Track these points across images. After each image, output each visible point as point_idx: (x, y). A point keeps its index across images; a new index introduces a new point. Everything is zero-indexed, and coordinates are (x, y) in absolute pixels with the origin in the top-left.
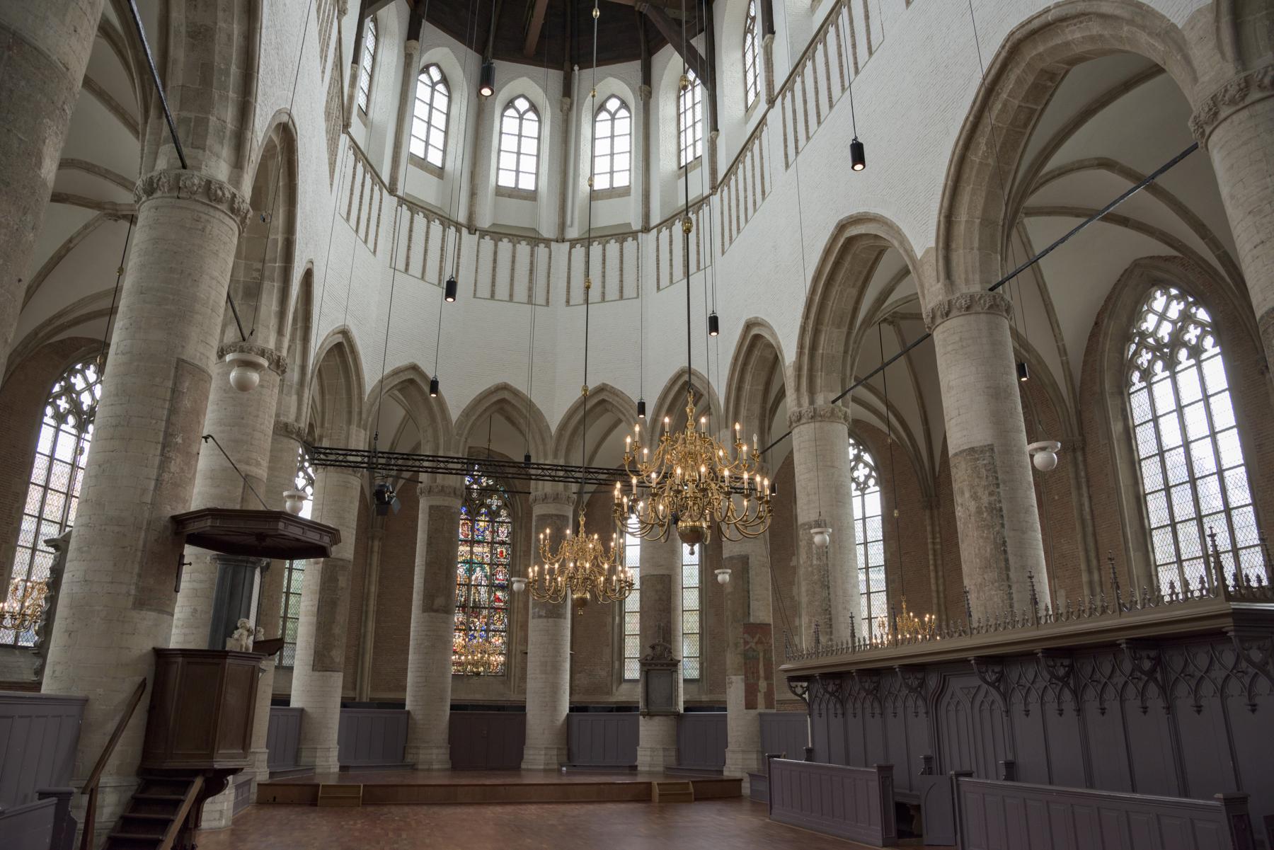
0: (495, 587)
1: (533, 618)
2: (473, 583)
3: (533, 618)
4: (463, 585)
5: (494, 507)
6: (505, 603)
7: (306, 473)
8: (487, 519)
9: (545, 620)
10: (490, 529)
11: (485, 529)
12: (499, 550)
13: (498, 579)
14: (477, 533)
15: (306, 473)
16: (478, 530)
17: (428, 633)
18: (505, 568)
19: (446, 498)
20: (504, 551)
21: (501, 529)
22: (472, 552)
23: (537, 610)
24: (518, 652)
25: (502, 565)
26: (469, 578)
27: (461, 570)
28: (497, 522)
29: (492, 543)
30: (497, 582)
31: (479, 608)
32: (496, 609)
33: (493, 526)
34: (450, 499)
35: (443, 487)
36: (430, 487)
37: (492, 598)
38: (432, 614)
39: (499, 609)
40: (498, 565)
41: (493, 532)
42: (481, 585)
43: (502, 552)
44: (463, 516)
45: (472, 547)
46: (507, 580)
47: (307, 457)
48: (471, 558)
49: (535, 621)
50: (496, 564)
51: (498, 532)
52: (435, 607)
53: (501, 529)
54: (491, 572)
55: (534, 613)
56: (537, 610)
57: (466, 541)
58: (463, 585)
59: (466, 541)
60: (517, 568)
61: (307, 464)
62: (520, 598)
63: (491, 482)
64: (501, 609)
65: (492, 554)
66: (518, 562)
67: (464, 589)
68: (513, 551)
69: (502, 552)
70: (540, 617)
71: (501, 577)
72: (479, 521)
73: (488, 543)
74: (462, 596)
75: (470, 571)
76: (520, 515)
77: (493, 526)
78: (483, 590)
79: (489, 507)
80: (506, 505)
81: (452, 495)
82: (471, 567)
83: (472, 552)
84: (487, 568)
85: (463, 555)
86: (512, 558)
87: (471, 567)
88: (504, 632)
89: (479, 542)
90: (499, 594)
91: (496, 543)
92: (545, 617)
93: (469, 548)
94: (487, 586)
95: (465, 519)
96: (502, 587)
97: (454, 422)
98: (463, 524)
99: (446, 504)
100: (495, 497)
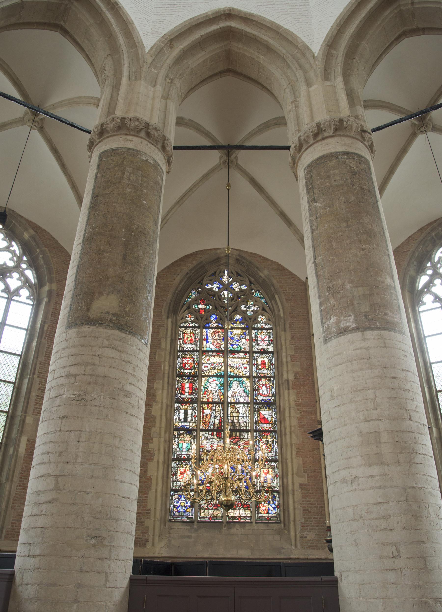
0: (258, 404)
1: (326, 340)
2: (230, 400)
3: (326, 340)
4: (217, 403)
5: (250, 313)
6: (274, 423)
7: (22, 274)
8: (243, 326)
9: (357, 335)
10: (247, 337)
11: (242, 336)
12: (259, 360)
13: (262, 395)
14: (230, 341)
15: (22, 274)
16: (232, 338)
17: (73, 370)
18: (270, 381)
19: (130, 138)
20: (267, 361)
21: (261, 337)
22: (226, 364)
23: (333, 320)
24: (297, 487)
25: (265, 377)
26: (225, 395)
27: (214, 385)
28: (255, 329)
29: (250, 353)
30: (260, 398)
31: (236, 431)
32: (262, 432)
33: (250, 334)
34: (135, 139)
35: (123, 119)
36: (102, 125)
37: (256, 418)
38: (87, 329)
39: (265, 431)
40: (260, 378)
41: (251, 340)
42: (239, 403)
43: (263, 363)
44: (213, 325)
45: (226, 358)
46: (273, 395)
47: (25, 258)
48: (226, 371)
49: (333, 343)
50: (257, 377)
51: (257, 340)
52: (93, 314)
53: (261, 337)
54: (252, 386)
55: (327, 331)
56: (333, 320)
57: (218, 352)
58: (217, 403)
59: (218, 352)
60: (285, 377)
61: (24, 266)
62: (293, 414)
63: (243, 287)
64: (269, 431)
65: (251, 365)
66: (285, 369)
67: (219, 408)
68: (278, 360)
69: (263, 363)
70: (343, 331)
71: (265, 392)
72: (232, 328)
73: (245, 353)
74: (216, 417)
75: (226, 386)
76: (282, 315)
77: (250, 334)
78: (241, 408)
79: (245, 312)
80: (264, 309)
81: (143, 134)
82: (226, 381)
83: (226, 364)
84: (247, 382)
85: (215, 368)
86: (278, 368)
87: (226, 381)
88: (275, 461)
89: (234, 352)
90: (265, 413)
91: (256, 352)
92: (356, 329)
93: (222, 360)
94: (248, 403)
95: (215, 328)
96: (267, 405)
97: (147, 50)
98: (214, 333)
99: (131, 145)
100: (250, 303)
